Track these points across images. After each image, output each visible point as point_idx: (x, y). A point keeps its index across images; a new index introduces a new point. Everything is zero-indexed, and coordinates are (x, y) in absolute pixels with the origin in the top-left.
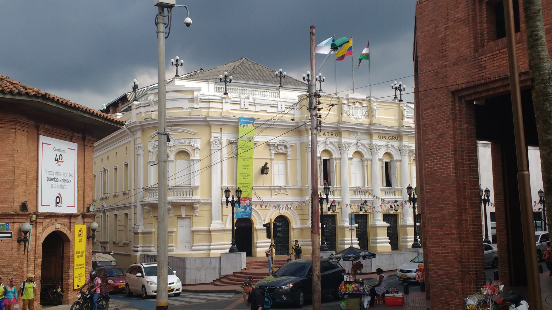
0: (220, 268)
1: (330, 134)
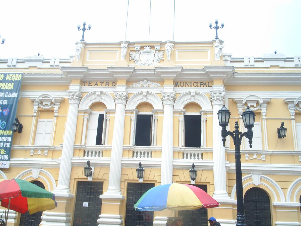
1: (104, 84)
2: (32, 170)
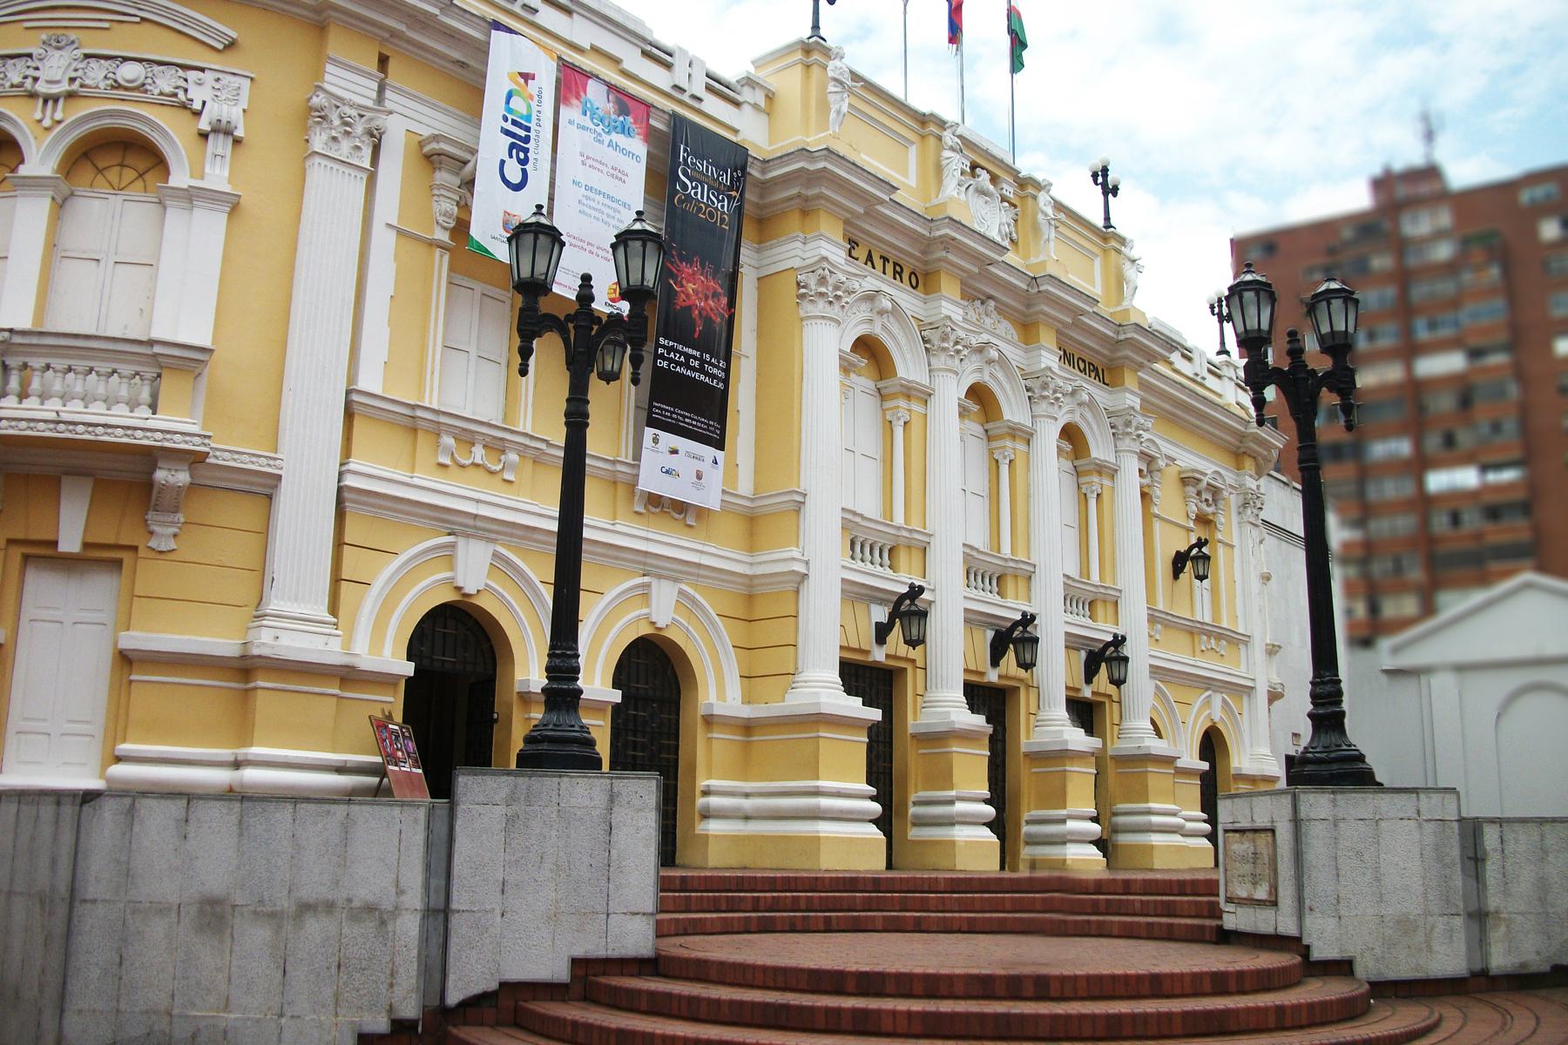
0: (439, 914)
1: (889, 268)
2: (648, 585)
